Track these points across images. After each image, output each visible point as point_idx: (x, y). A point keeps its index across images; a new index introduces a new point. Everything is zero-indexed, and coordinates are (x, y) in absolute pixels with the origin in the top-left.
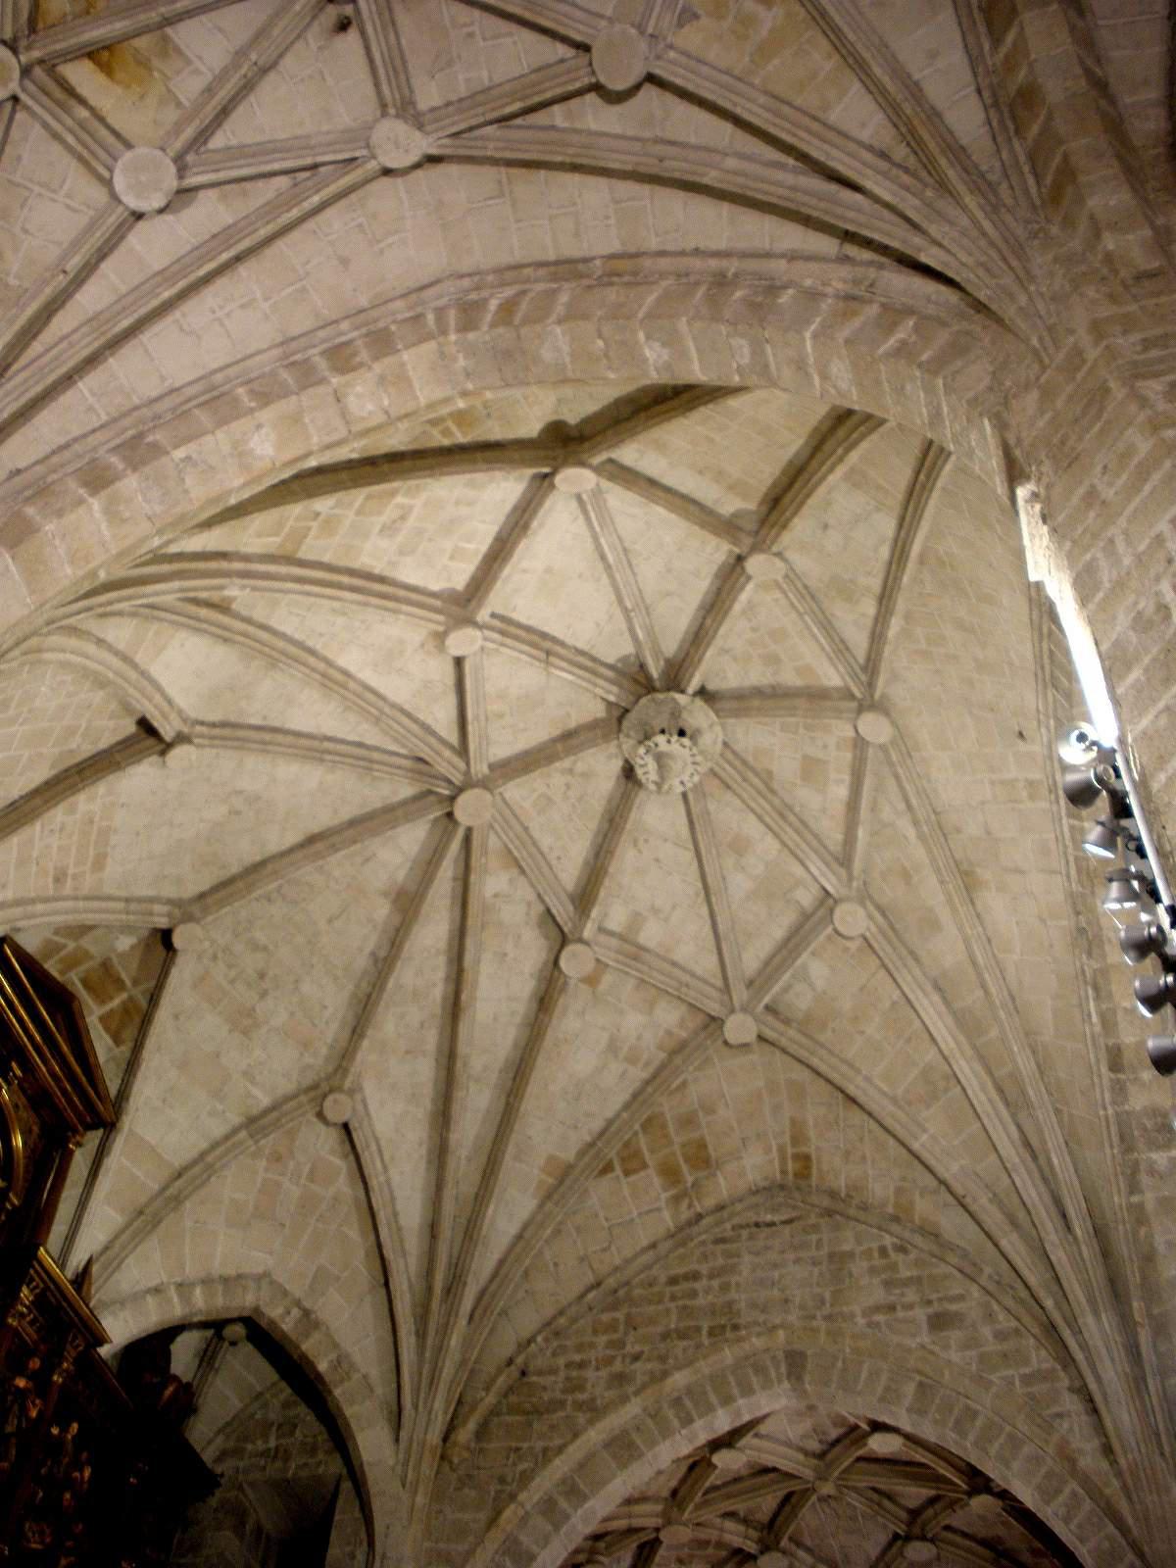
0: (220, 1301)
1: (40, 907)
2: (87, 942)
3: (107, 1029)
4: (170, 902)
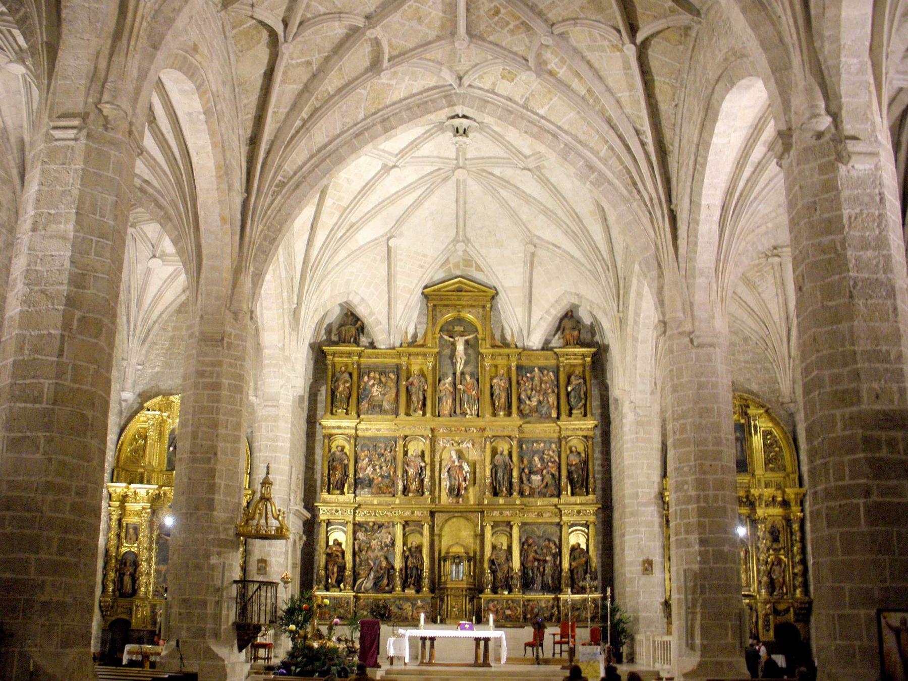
0: (559, 308)
2: (452, 261)
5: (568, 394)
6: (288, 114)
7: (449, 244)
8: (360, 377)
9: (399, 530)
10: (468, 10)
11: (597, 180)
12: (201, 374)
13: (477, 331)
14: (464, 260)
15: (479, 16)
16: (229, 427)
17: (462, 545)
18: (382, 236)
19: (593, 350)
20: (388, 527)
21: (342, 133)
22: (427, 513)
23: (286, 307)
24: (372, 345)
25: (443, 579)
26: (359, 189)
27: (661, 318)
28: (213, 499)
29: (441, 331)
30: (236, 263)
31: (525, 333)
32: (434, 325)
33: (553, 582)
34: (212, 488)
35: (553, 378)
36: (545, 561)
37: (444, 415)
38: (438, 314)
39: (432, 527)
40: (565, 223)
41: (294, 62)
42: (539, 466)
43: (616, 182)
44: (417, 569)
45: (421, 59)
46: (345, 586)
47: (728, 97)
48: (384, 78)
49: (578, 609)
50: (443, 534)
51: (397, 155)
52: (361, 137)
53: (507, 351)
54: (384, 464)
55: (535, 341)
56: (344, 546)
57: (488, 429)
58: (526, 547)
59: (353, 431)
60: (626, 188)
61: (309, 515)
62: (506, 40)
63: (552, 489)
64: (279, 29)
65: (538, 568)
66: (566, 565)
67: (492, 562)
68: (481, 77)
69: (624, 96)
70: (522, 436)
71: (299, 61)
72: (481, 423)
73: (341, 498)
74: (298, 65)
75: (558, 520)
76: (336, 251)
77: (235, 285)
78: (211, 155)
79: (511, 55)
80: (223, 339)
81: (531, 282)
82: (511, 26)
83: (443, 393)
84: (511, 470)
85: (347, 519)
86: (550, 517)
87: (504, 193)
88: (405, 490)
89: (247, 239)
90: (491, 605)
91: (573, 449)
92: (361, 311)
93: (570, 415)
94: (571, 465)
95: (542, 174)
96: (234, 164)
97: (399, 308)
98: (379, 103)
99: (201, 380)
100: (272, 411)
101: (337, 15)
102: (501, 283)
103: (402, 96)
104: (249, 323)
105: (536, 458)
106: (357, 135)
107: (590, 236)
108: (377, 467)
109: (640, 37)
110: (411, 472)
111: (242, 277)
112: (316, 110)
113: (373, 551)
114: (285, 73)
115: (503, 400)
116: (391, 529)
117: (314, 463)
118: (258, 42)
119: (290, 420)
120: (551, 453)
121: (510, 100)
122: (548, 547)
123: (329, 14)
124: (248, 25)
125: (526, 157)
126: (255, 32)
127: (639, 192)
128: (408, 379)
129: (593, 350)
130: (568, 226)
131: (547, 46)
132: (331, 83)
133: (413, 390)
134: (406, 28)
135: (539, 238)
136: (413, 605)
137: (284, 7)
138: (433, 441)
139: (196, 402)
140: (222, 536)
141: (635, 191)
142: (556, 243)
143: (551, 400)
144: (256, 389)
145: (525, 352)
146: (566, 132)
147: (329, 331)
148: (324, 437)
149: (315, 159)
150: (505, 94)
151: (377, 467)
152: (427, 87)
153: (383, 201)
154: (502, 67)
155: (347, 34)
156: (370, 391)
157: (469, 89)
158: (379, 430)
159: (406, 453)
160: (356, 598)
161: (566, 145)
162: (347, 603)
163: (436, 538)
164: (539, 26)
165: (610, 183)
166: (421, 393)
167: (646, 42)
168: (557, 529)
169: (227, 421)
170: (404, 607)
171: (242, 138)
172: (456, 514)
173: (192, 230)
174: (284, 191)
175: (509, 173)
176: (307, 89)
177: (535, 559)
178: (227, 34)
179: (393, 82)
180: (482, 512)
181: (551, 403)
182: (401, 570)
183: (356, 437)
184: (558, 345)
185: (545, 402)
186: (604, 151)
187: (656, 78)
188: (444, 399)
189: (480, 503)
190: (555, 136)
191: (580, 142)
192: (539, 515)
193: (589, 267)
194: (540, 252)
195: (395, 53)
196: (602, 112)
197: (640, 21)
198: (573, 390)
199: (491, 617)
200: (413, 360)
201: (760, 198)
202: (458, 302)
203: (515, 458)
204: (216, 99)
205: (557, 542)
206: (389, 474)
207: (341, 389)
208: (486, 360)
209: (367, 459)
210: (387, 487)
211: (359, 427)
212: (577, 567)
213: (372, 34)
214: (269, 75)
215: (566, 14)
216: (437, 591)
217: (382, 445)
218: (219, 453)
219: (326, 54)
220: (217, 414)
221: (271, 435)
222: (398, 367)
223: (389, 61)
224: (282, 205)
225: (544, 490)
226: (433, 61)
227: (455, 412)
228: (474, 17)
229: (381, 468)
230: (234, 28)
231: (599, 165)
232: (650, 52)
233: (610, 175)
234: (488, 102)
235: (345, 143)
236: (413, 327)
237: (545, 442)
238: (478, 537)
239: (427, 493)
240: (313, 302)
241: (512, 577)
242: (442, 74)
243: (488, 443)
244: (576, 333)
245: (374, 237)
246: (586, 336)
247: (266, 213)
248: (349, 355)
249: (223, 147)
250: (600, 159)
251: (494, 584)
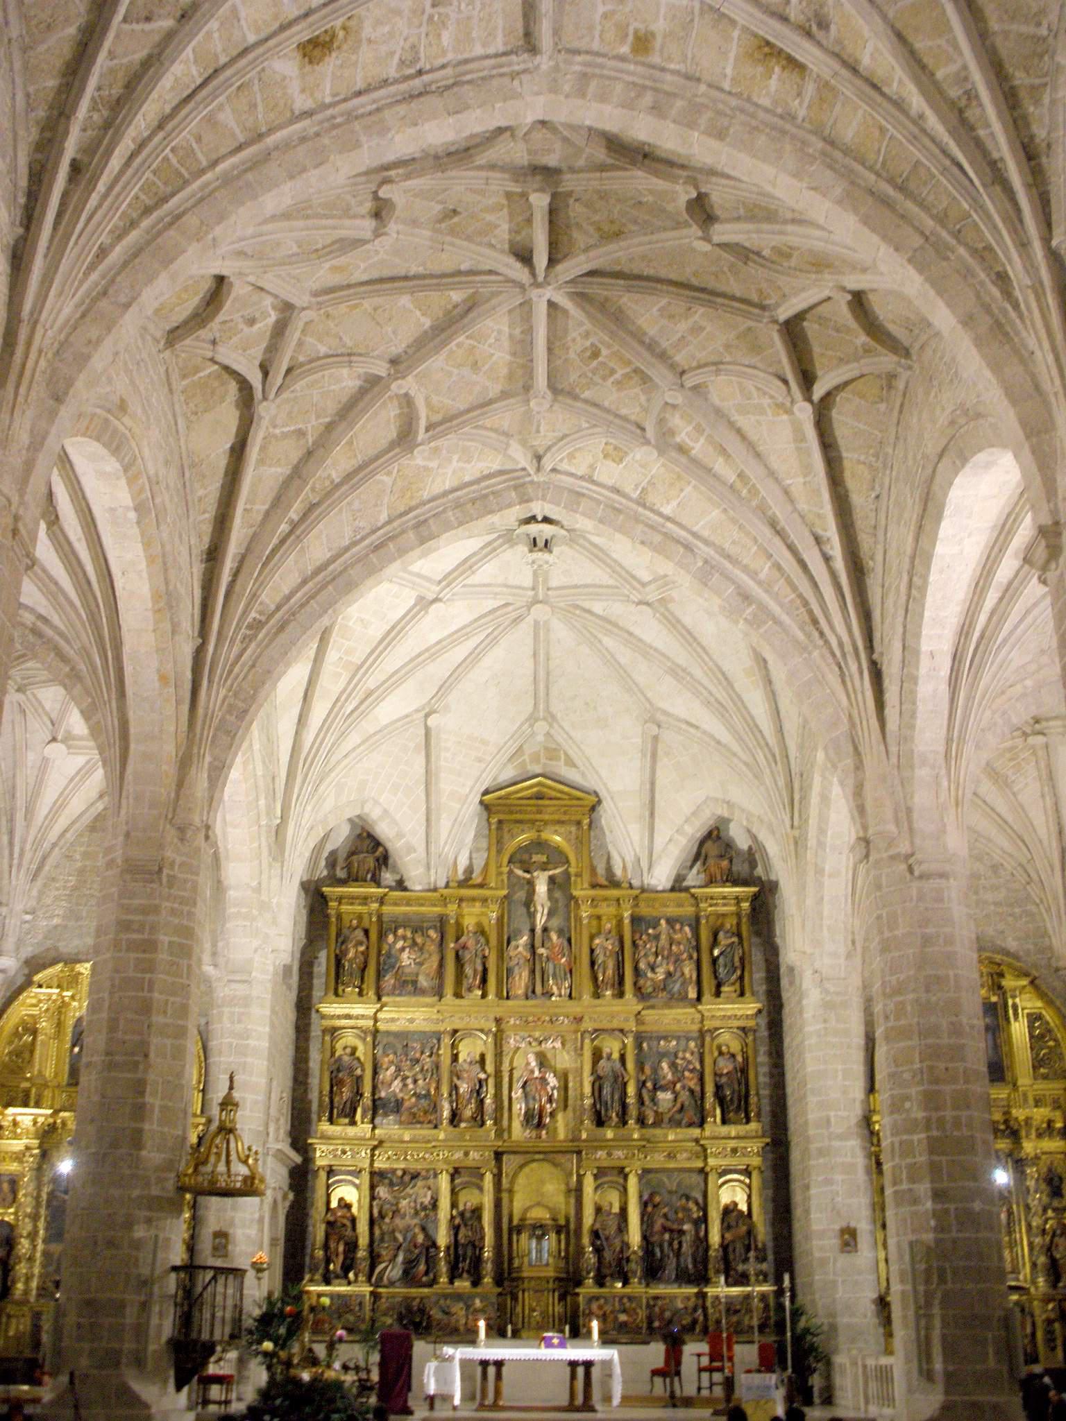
1: (484, 775)
2: (528, 750)
4: (527, 720)
5: (714, 961)
6: (267, 514)
7: (522, 724)
8: (382, 936)
9: (444, 1182)
10: (550, 350)
11: (755, 615)
12: (125, 926)
13: (568, 862)
14: (546, 749)
15: (566, 360)
16: (169, 1012)
17: (547, 1207)
18: (417, 711)
19: (754, 889)
20: (426, 1178)
21: (355, 544)
22: (489, 1154)
23: (263, 823)
24: (401, 885)
25: (516, 1263)
26: (379, 636)
27: (861, 834)
28: (140, 1131)
30: (183, 748)
31: (644, 864)
32: (499, 852)
33: (695, 1266)
34: (140, 1111)
35: (689, 935)
36: (681, 1232)
37: (516, 997)
38: (506, 836)
39: (498, 1178)
40: (706, 688)
41: (277, 431)
42: (670, 1076)
43: (785, 618)
44: (474, 1247)
45: (476, 427)
46: (356, 1275)
47: (957, 481)
48: (420, 458)
49: (736, 1312)
50: (516, 1188)
51: (440, 582)
52: (382, 551)
53: (615, 893)
54: (420, 1076)
55: (661, 877)
56: (354, 1210)
57: (586, 1018)
58: (650, 1209)
59: (371, 1023)
60: (802, 629)
61: (298, 1159)
62: (609, 395)
63: (691, 1114)
64: (255, 378)
65: (671, 1244)
66: (715, 1238)
67: (595, 1234)
68: (571, 456)
69: (796, 483)
70: (642, 1028)
71: (286, 429)
72: (574, 1008)
73: (351, 1131)
74: (285, 436)
75: (700, 1164)
76: (343, 735)
77: (180, 784)
78: (145, 575)
79: (617, 421)
80: (160, 870)
81: (653, 784)
82: (617, 376)
83: (512, 963)
84: (625, 1084)
85: (361, 1165)
86: (689, 1159)
87: (608, 641)
88: (455, 1118)
89: (200, 711)
90: (594, 1306)
91: (724, 1049)
92: (384, 830)
93: (718, 994)
94: (721, 1075)
95: (667, 609)
96: (182, 591)
97: (444, 826)
98: (412, 498)
99: (124, 936)
100: (240, 989)
101: (346, 359)
102: (605, 784)
103: (447, 486)
104: (203, 844)
105: (665, 1065)
106: (377, 548)
107: (746, 708)
108: (409, 1081)
109: (818, 391)
110: (464, 1088)
111: (193, 770)
112: (312, 507)
113: (403, 1217)
114: (263, 448)
115: (610, 972)
116: (431, 1181)
117: (306, 1075)
118: (222, 399)
119: (268, 1004)
120: (688, 1055)
121: (618, 491)
122: (686, 1210)
123: (333, 356)
124: (207, 371)
125: (644, 585)
126: (216, 384)
127: (822, 634)
128: (458, 939)
129: (754, 889)
130: (710, 693)
131: (674, 407)
132: (337, 464)
133: (467, 956)
134: (454, 378)
135: (665, 713)
136: (468, 1307)
137: (264, 345)
138: (499, 1039)
139: (117, 971)
140: (155, 1191)
141: (816, 634)
142: (694, 721)
143: (687, 971)
144: (214, 954)
145: (645, 895)
146: (706, 542)
147: (332, 862)
148: (324, 1031)
149: (311, 584)
150: (610, 482)
151: (409, 1081)
152: (486, 472)
153: (419, 655)
154: (604, 441)
155: (361, 388)
156: (398, 959)
157: (553, 475)
158: (411, 1021)
159: (455, 1058)
160: (375, 1296)
161: (706, 562)
162: (360, 1304)
163: (505, 1196)
164: (659, 373)
165: (777, 621)
166: (479, 961)
167: (828, 397)
168: (700, 1179)
169: (167, 1001)
170: (453, 1310)
171: (194, 552)
172: (537, 1157)
173: (114, 696)
174: (260, 636)
175: (617, 610)
176: (297, 474)
177: (665, 1229)
178: (174, 387)
179: (433, 464)
180: (579, 1153)
181: (688, 976)
182: (448, 1248)
183: (376, 1032)
184: (698, 883)
185: (678, 974)
186: (765, 571)
187: (845, 454)
188: (516, 970)
189: (576, 1139)
190: (688, 547)
191: (728, 557)
192: (671, 1156)
193: (744, 757)
194: (668, 736)
195: (436, 418)
196: (762, 509)
197: (817, 365)
198: (721, 954)
199: (595, 1325)
200: (466, 908)
201: (1012, 640)
202: (538, 817)
203: (630, 1065)
204: (155, 488)
205: (700, 1200)
206: (429, 1091)
207: (351, 954)
208: (583, 908)
209: (393, 1068)
210: (426, 1112)
211: (380, 1015)
212: (733, 1241)
213: (400, 387)
214: (238, 451)
215: (702, 356)
216: (506, 1283)
217: (417, 1046)
218: (152, 1055)
219: (328, 420)
220: (151, 990)
221: (239, 1027)
222: (442, 921)
223: (427, 430)
224: (258, 657)
225: (678, 1117)
226: (495, 431)
227: (533, 992)
228: (559, 362)
229: (415, 1081)
230: (184, 377)
231: (757, 591)
232: (834, 413)
233: (776, 609)
234: (583, 495)
235: (359, 561)
236: (467, 854)
237: (678, 1038)
238: (573, 1194)
239: (489, 1123)
240: (307, 815)
241: (628, 1260)
242: (511, 452)
243: (587, 1041)
244: (725, 863)
245: (404, 713)
246: (740, 868)
247: (230, 672)
248: (365, 900)
249: (165, 563)
250: (760, 583)
251: (599, 1270)
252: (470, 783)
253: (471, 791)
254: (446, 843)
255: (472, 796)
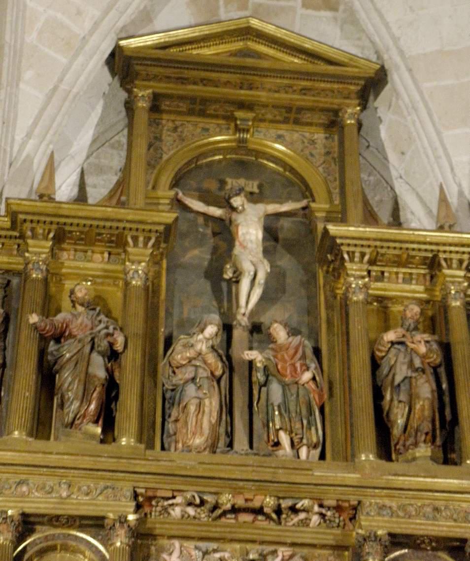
3: (317, 8)
13: (306, 191)
29: (176, 183)
38: (168, 138)
57: (370, 501)
188: (191, 390)
200: (70, 260)
236: (75, 178)
252: (93, 12)
253: (91, 33)
254: (29, 135)
255: (95, 38)
